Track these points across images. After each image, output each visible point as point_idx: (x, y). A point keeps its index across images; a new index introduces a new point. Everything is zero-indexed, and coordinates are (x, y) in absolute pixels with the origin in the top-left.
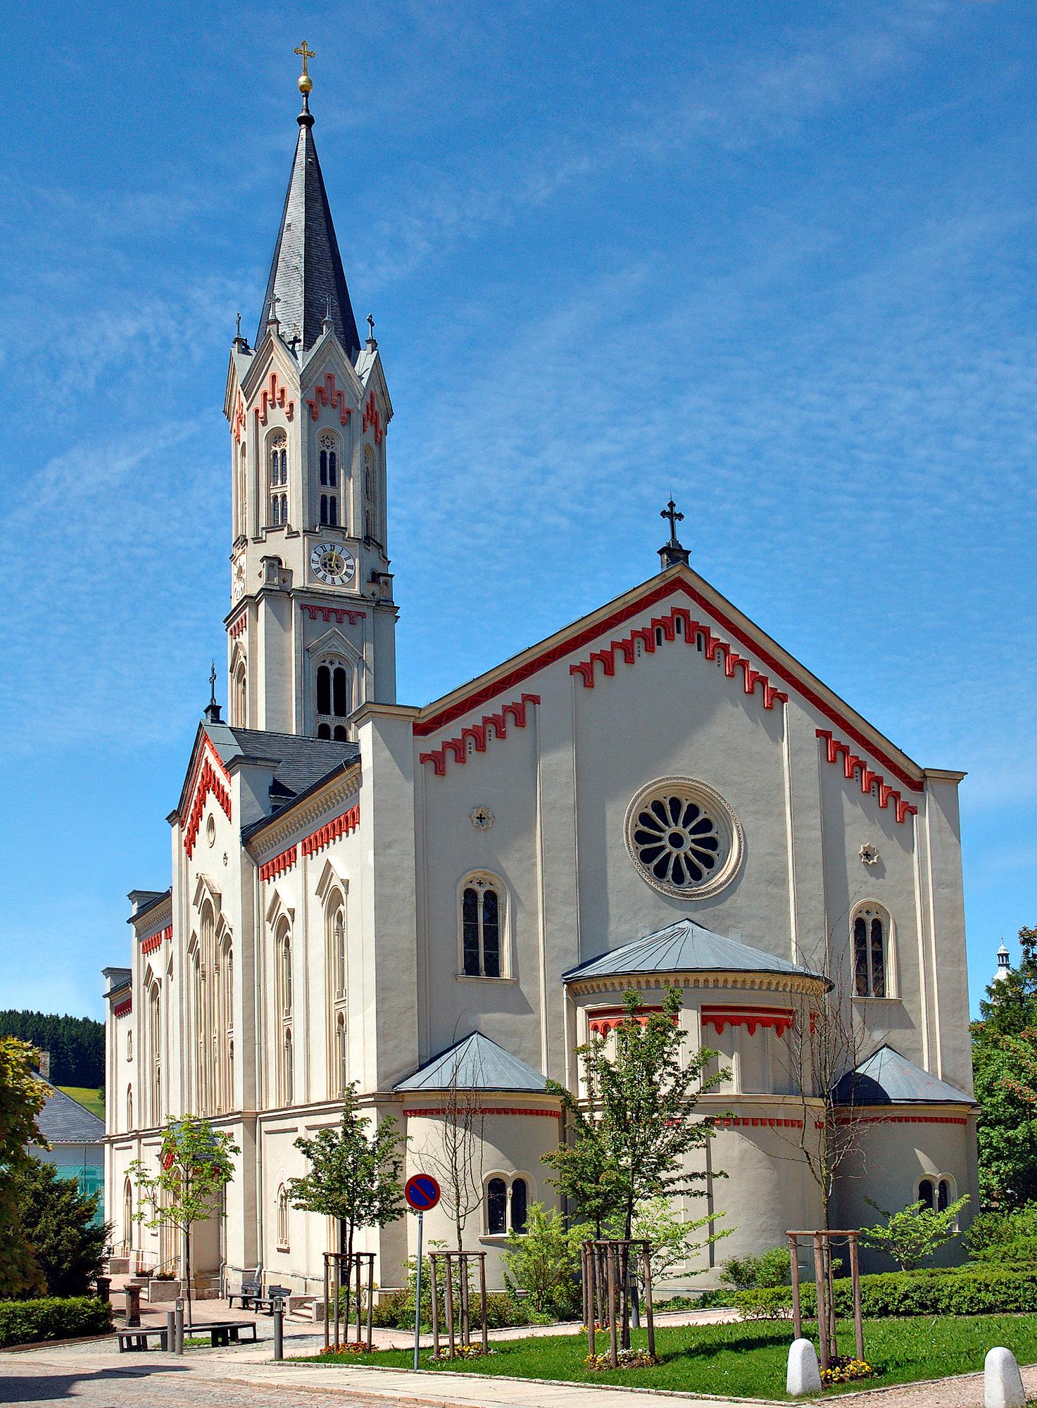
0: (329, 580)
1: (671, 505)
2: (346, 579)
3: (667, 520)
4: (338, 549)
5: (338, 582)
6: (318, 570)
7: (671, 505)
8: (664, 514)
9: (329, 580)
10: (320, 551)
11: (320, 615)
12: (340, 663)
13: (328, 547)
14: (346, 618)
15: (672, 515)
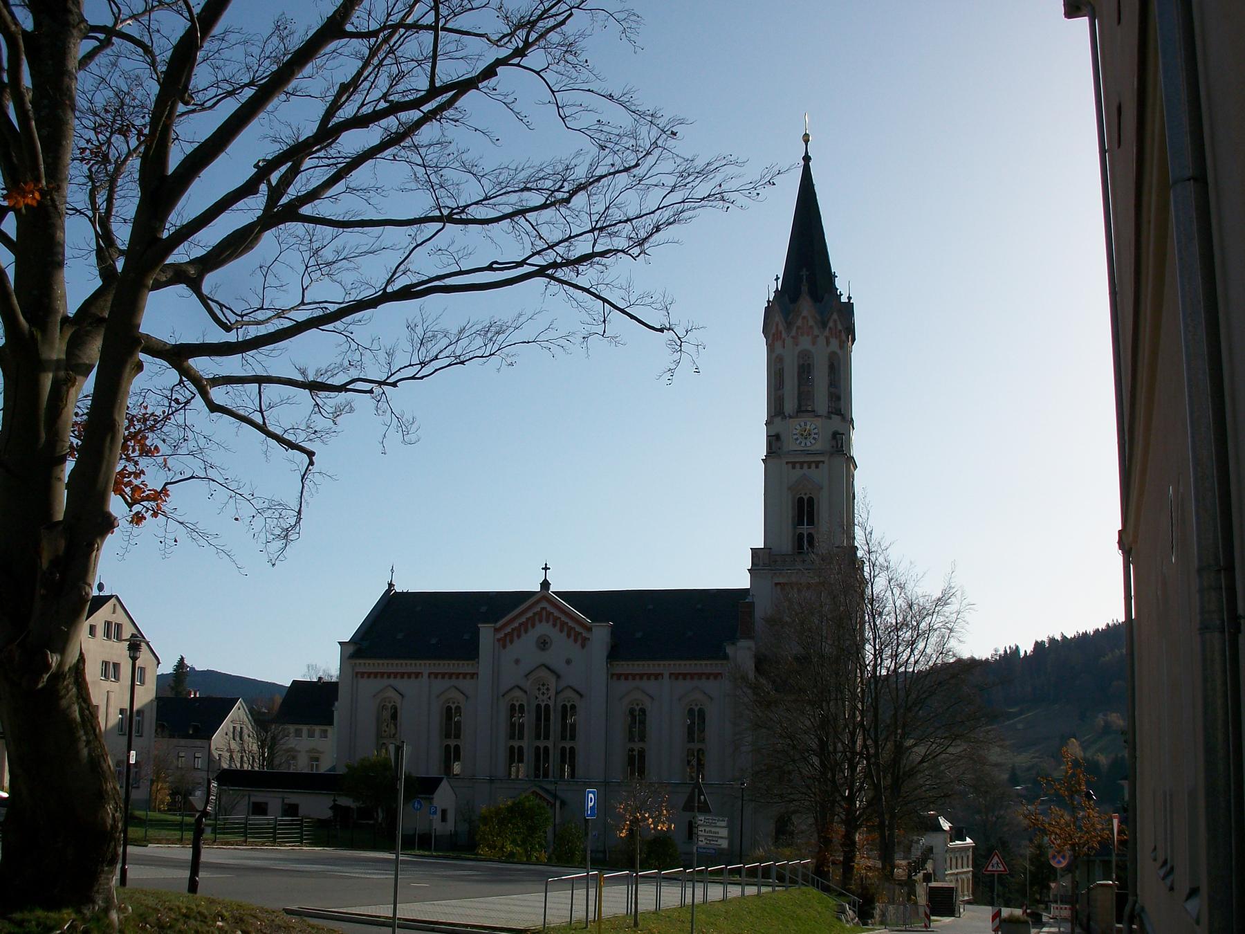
0: (803, 444)
1: (546, 564)
2: (813, 441)
3: (544, 571)
4: (809, 424)
5: (808, 444)
6: (797, 439)
7: (546, 564)
8: (543, 569)
9: (803, 444)
10: (798, 427)
11: (798, 466)
12: (810, 494)
13: (802, 424)
14: (813, 466)
15: (546, 568)
